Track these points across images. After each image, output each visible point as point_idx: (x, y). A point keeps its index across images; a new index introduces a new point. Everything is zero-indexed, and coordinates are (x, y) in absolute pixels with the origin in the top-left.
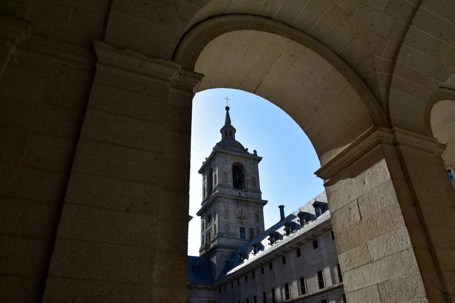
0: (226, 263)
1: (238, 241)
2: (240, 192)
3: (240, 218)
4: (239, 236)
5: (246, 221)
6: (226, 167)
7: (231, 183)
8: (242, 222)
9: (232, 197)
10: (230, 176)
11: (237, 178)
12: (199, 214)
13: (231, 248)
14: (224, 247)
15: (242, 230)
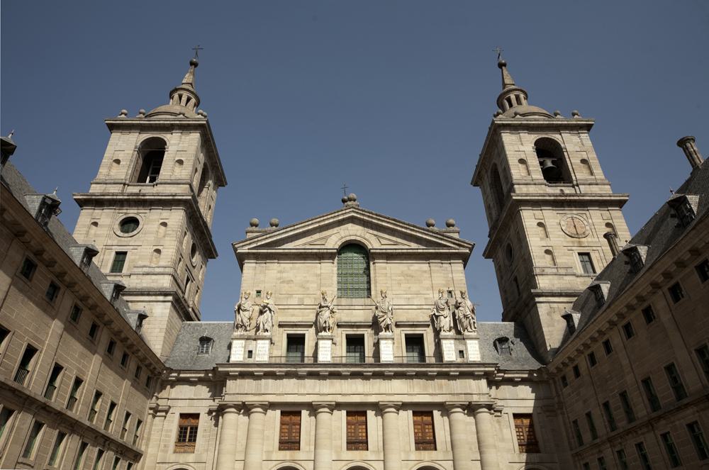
0: (564, 323)
1: (579, 280)
2: (563, 188)
3: (575, 236)
4: (580, 270)
5: (589, 239)
6: (522, 148)
7: (538, 175)
8: (579, 242)
9: (548, 198)
10: (534, 161)
11: (549, 164)
12: (488, 254)
13: (567, 295)
14: (553, 295)
15: (586, 256)
